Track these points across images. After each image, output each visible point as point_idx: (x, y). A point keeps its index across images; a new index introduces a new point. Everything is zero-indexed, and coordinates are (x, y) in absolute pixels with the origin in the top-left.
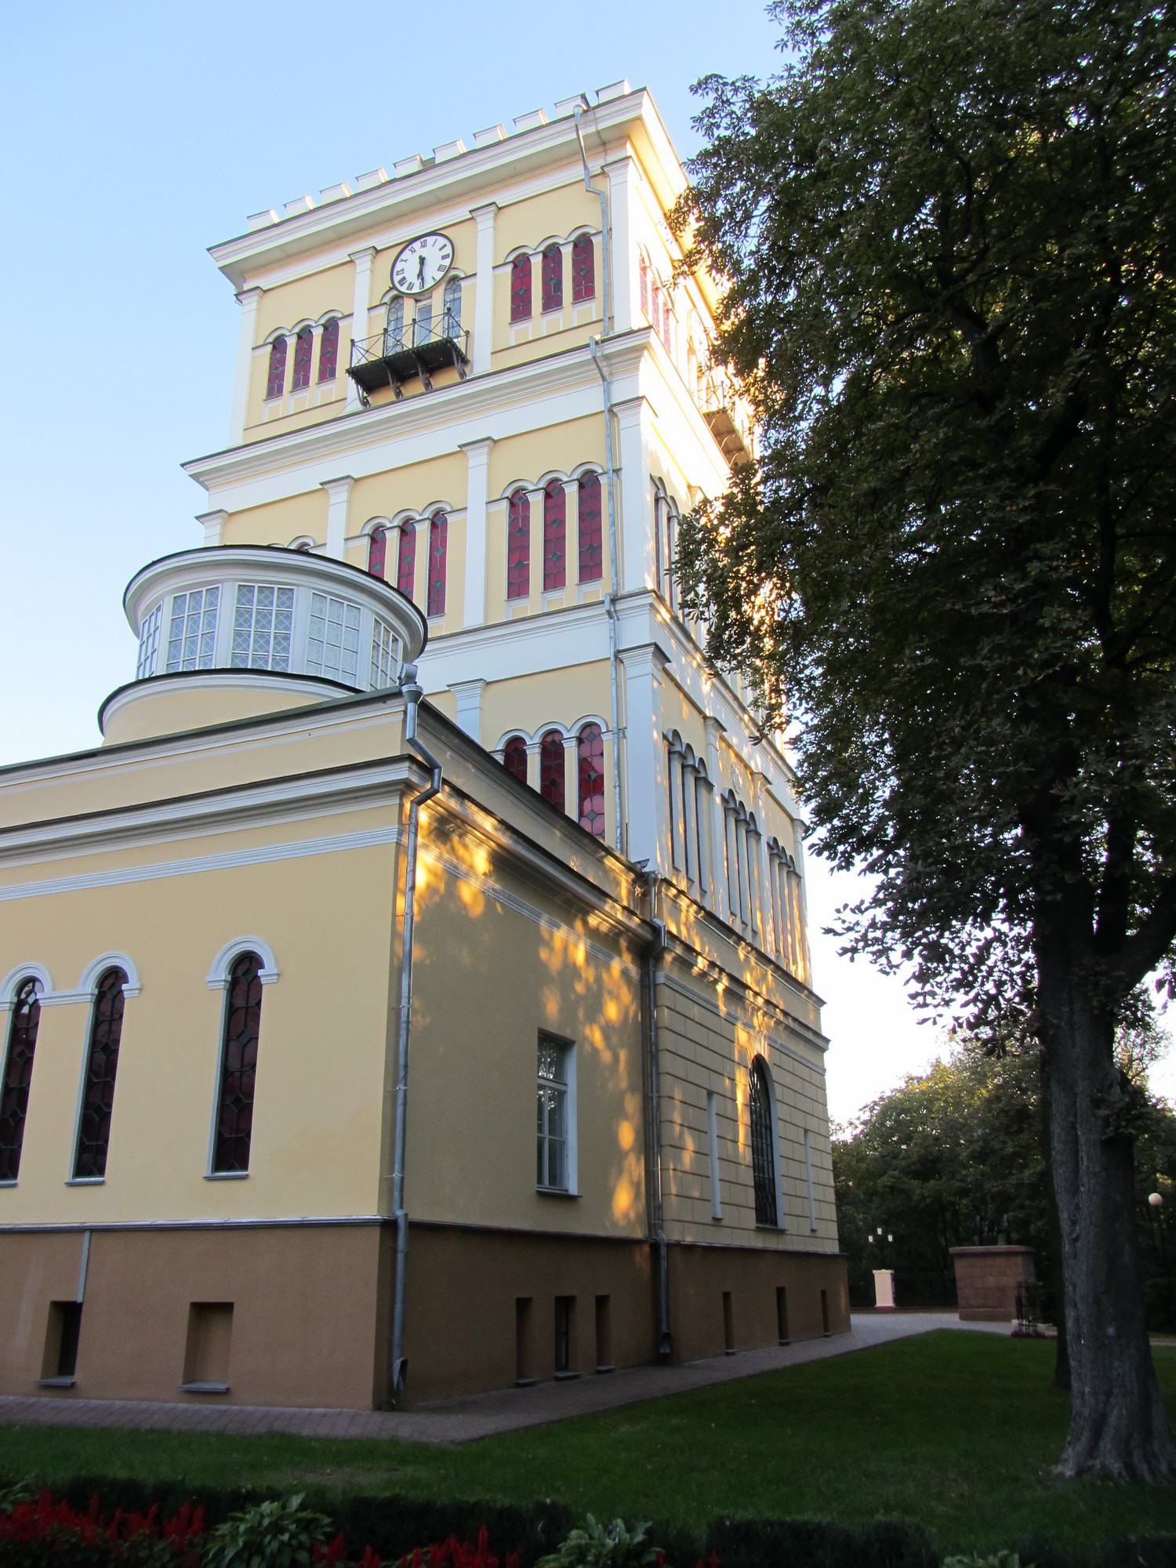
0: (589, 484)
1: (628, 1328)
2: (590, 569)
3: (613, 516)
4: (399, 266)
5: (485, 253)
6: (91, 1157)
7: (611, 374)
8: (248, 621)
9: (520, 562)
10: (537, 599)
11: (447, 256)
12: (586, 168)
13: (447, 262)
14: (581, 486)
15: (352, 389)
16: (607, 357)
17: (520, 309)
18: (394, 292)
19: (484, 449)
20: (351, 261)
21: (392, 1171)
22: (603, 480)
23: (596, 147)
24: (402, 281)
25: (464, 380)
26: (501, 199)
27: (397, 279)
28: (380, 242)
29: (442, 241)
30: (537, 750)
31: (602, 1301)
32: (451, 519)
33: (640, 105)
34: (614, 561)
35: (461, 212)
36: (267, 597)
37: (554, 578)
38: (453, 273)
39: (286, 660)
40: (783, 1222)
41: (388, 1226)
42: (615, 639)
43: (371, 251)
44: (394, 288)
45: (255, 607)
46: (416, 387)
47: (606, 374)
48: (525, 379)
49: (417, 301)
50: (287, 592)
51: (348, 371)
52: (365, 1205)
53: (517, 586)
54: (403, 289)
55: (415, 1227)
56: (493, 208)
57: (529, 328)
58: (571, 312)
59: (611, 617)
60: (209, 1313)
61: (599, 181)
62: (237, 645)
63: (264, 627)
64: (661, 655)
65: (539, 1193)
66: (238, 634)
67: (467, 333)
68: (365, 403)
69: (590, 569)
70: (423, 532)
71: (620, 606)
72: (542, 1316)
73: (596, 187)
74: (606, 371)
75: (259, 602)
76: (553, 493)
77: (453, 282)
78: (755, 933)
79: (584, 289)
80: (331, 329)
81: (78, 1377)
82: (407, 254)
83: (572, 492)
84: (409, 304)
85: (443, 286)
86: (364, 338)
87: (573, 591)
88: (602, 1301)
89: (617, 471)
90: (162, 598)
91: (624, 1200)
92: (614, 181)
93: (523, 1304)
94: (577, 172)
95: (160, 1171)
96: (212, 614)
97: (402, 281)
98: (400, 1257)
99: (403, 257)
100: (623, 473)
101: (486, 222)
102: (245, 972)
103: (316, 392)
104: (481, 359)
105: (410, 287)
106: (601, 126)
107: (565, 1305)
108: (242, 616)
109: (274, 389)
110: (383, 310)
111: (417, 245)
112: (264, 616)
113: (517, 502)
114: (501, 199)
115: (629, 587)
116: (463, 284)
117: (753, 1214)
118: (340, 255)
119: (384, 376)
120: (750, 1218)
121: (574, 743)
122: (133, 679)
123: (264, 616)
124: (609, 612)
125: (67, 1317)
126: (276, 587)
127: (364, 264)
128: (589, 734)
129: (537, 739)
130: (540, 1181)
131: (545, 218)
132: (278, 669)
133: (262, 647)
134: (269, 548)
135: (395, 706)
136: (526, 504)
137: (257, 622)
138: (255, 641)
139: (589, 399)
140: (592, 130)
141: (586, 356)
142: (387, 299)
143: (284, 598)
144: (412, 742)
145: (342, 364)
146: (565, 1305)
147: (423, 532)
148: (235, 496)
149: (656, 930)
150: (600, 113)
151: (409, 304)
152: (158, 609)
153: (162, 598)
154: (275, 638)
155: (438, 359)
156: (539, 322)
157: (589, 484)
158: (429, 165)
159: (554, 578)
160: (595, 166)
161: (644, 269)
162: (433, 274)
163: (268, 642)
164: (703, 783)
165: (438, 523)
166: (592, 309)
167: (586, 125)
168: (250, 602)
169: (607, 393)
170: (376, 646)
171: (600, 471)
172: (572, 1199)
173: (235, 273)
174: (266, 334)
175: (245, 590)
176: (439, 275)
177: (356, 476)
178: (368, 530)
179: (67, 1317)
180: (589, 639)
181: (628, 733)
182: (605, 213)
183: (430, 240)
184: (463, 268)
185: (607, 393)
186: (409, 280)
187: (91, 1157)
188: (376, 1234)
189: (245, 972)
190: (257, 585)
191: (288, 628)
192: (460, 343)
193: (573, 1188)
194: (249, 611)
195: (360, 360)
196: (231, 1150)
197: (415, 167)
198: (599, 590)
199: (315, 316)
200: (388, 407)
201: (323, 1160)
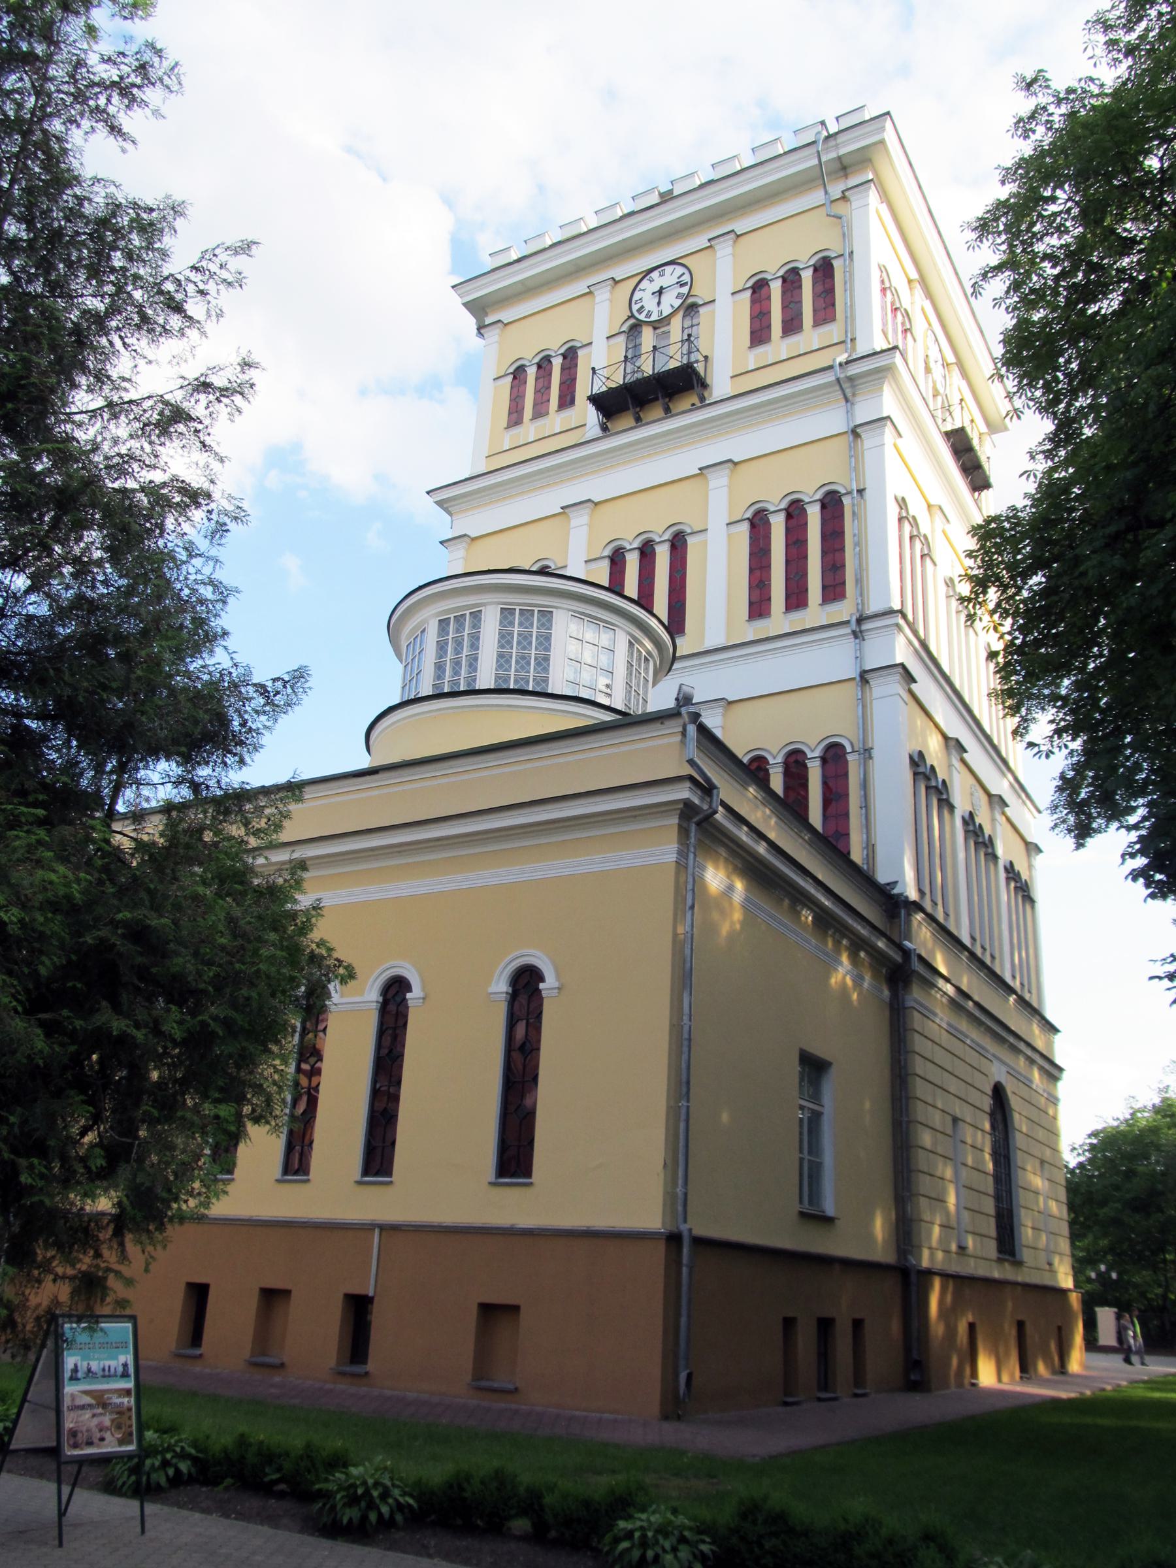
1: (882, 1356)
2: (833, 591)
4: (637, 296)
5: (724, 278)
6: (378, 1158)
7: (854, 395)
8: (510, 643)
9: (761, 581)
10: (779, 620)
11: (686, 284)
12: (826, 192)
14: (824, 507)
15: (592, 416)
16: (850, 379)
17: (759, 335)
18: (632, 321)
19: (725, 471)
20: (590, 293)
21: (675, 1184)
22: (846, 501)
23: (836, 172)
24: (640, 310)
25: (703, 402)
26: (740, 226)
27: (635, 308)
28: (619, 272)
29: (679, 270)
30: (780, 769)
31: (858, 1324)
32: (691, 541)
33: (883, 129)
34: (859, 581)
35: (701, 241)
36: (527, 619)
37: (796, 599)
38: (691, 300)
39: (546, 680)
40: (1026, 1255)
41: (673, 1239)
42: (859, 658)
43: (611, 282)
44: (632, 316)
45: (516, 629)
46: (657, 411)
47: (849, 395)
48: (764, 400)
49: (655, 329)
50: (546, 615)
51: (589, 398)
52: (650, 1217)
53: (758, 607)
54: (642, 317)
55: (700, 1242)
56: (732, 236)
57: (766, 353)
58: (810, 336)
59: (856, 637)
60: (493, 1314)
61: (840, 203)
62: (499, 666)
63: (524, 648)
64: (910, 678)
65: (802, 1214)
66: (500, 656)
67: (706, 357)
68: (604, 428)
69: (833, 591)
70: (663, 556)
71: (866, 626)
72: (806, 1340)
73: (837, 211)
74: (849, 392)
75: (521, 624)
76: (795, 512)
77: (690, 309)
78: (993, 957)
79: (826, 311)
80: (570, 356)
81: (371, 1366)
82: (645, 284)
83: (814, 514)
85: (681, 313)
86: (604, 366)
87: (815, 612)
88: (858, 1324)
89: (861, 492)
90: (425, 621)
91: (879, 1227)
92: (855, 204)
93: (789, 1323)
94: (816, 197)
95: (445, 1174)
96: (475, 639)
98: (685, 1270)
99: (641, 286)
100: (868, 494)
101: (724, 250)
102: (526, 981)
103: (556, 420)
104: (720, 384)
105: (649, 315)
106: (842, 152)
107: (825, 1326)
108: (505, 638)
109: (515, 417)
110: (622, 339)
111: (655, 275)
112: (525, 638)
113: (758, 523)
114: (740, 226)
115: (873, 607)
118: (580, 287)
119: (624, 403)
120: (991, 1249)
121: (818, 763)
122: (398, 701)
123: (525, 638)
124: (854, 633)
125: (359, 1308)
126: (536, 609)
127: (602, 295)
128: (834, 755)
129: (780, 759)
130: (801, 1202)
131: (785, 241)
132: (538, 689)
133: (522, 667)
134: (511, 571)
135: (674, 726)
136: (767, 524)
137: (519, 643)
138: (517, 662)
139: (830, 420)
140: (833, 155)
141: (828, 377)
142: (625, 328)
143: (544, 620)
144: (691, 762)
145: (583, 389)
146: (825, 1326)
147: (663, 556)
148: (476, 522)
149: (906, 953)
150: (841, 139)
152: (424, 631)
153: (425, 621)
154: (536, 659)
155: (678, 386)
156: (779, 346)
157: (832, 504)
158: (667, 197)
159: (796, 599)
160: (836, 190)
161: (884, 290)
162: (671, 301)
163: (529, 664)
164: (946, 804)
165: (678, 544)
166: (832, 331)
167: (827, 150)
168: (512, 624)
170: (630, 665)
171: (843, 491)
172: (828, 1220)
173: (478, 308)
174: (507, 366)
175: (507, 613)
177: (596, 500)
178: (607, 552)
179: (359, 1308)
180: (834, 659)
181: (875, 753)
182: (846, 236)
183: (669, 269)
184: (701, 293)
186: (647, 308)
187: (378, 1158)
188: (661, 1247)
189: (526, 981)
190: (518, 608)
191: (548, 649)
192: (700, 367)
193: (830, 1209)
194: (511, 634)
195: (599, 387)
196: (515, 1158)
197: (654, 199)
198: (843, 610)
199: (555, 344)
200: (629, 435)
201: (607, 1168)
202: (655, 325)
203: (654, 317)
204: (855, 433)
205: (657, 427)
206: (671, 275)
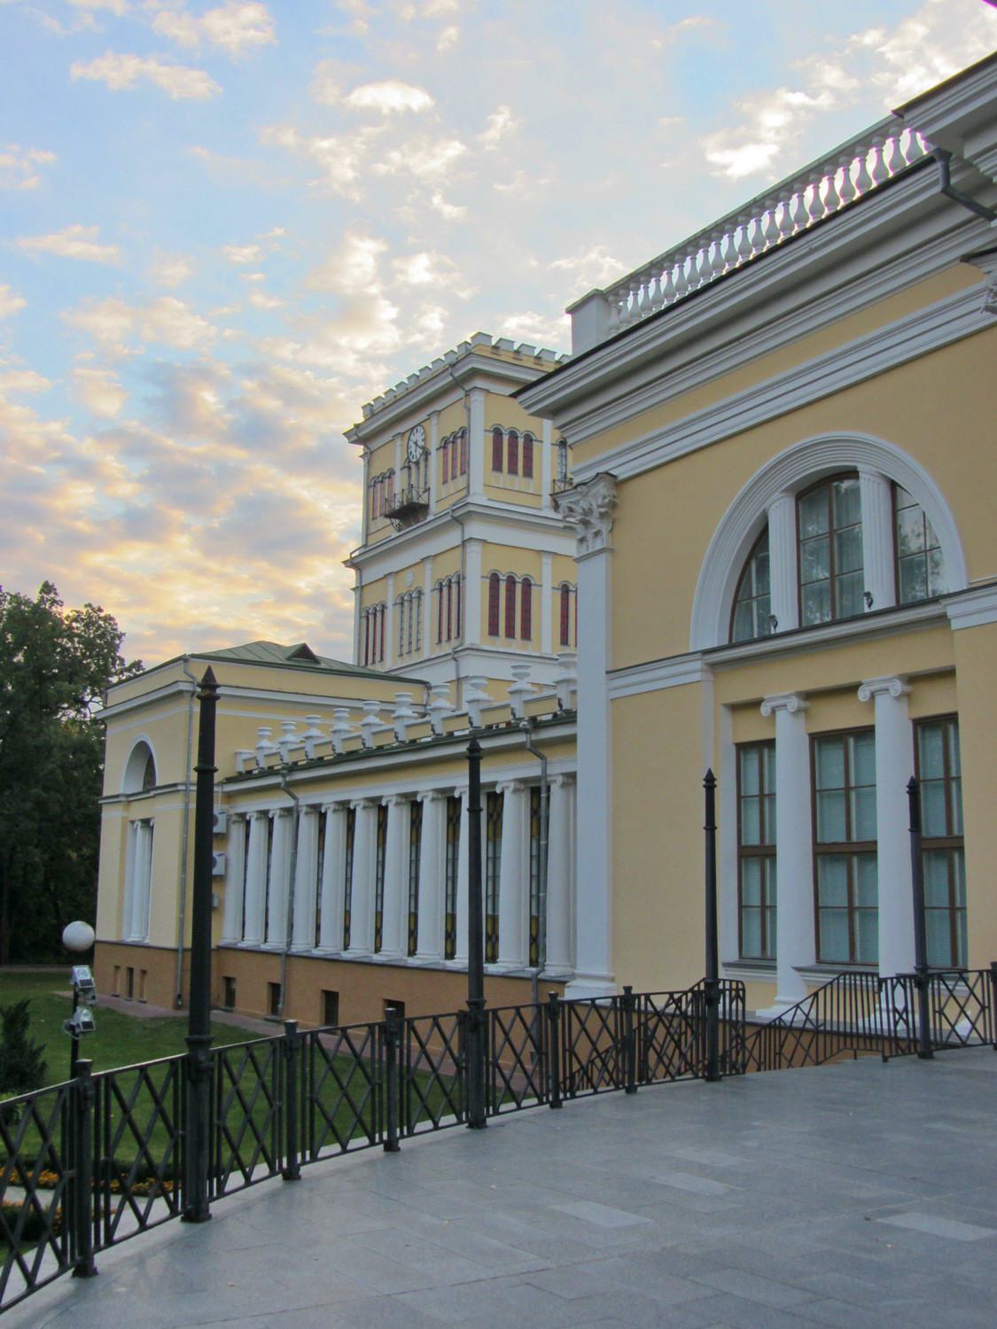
35: (422, 416)
44: (408, 458)
77: (426, 453)
84: (413, 466)
92: (472, 399)
94: (459, 394)
101: (434, 420)
114: (438, 406)
127: (398, 442)
131: (450, 422)
151: (413, 466)
162: (420, 451)
183: (419, 428)
192: (422, 501)
202: (417, 463)
204: (464, 543)
205: (416, 530)
206: (418, 437)
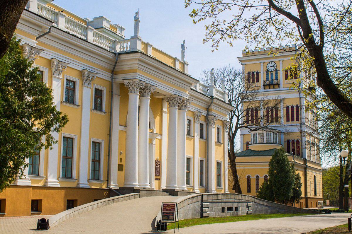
0: (297, 107)
2: (298, 120)
3: (301, 113)
4: (268, 66)
13: (275, 67)
22: (299, 107)
24: (269, 69)
27: (268, 68)
29: (274, 64)
31: (303, 202)
37: (293, 120)
54: (269, 70)
76: (292, 107)
84: (270, 73)
88: (303, 202)
97: (269, 69)
101: (281, 62)
105: (270, 70)
110: (265, 73)
111: (270, 63)
116: (278, 71)
117: (314, 194)
118: (259, 62)
120: (313, 194)
129: (291, 141)
136: (289, 109)
151: (270, 73)
159: (293, 120)
169: (300, 95)
176: (274, 69)
183: (273, 63)
184: (278, 68)
185: (300, 95)
202: (271, 72)
203: (271, 71)
